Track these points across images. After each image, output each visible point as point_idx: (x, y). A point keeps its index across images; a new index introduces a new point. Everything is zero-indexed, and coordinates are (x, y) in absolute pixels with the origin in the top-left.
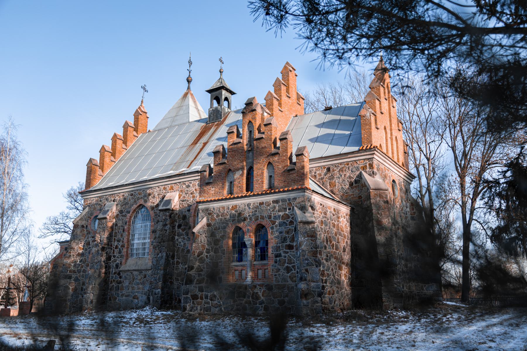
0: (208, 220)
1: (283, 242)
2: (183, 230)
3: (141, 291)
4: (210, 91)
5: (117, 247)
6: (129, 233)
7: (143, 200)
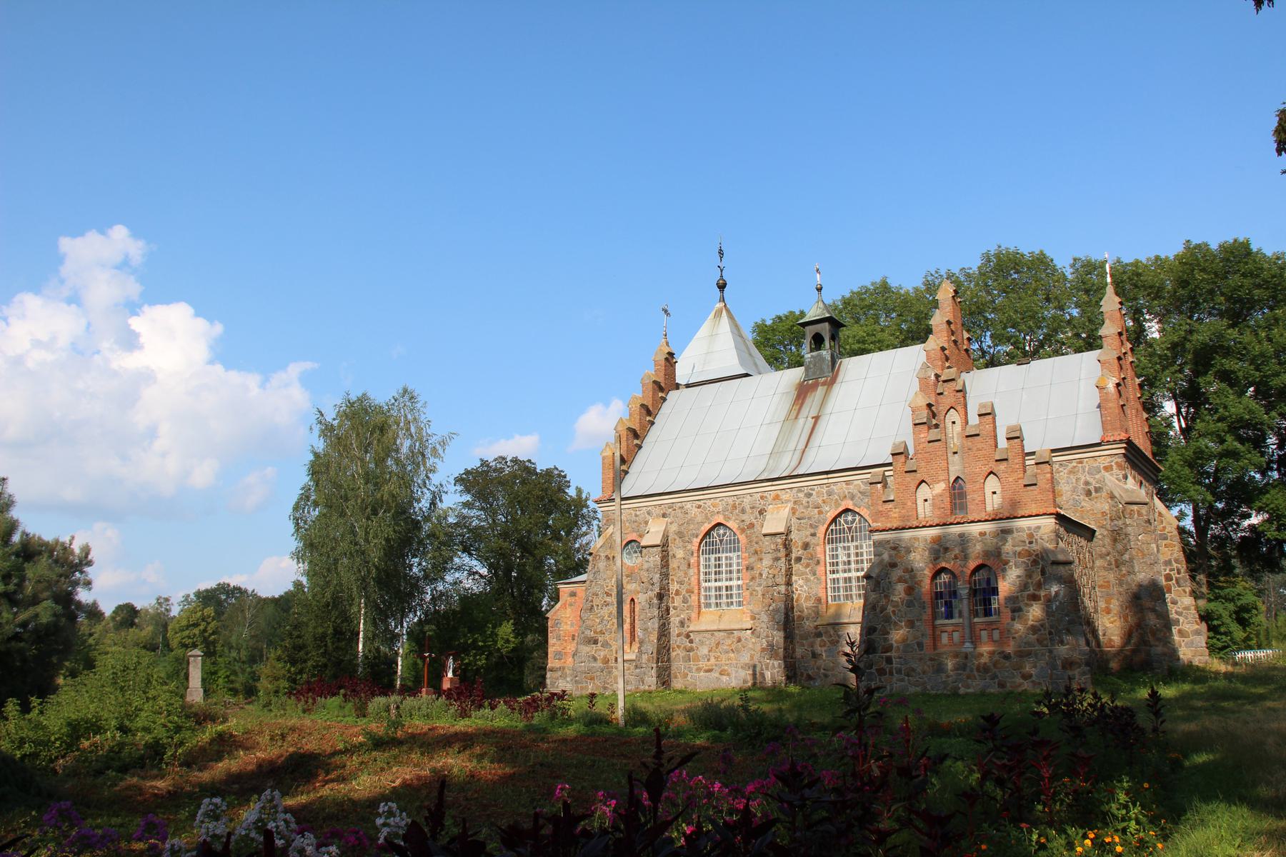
2: (808, 565)
5: (677, 593)
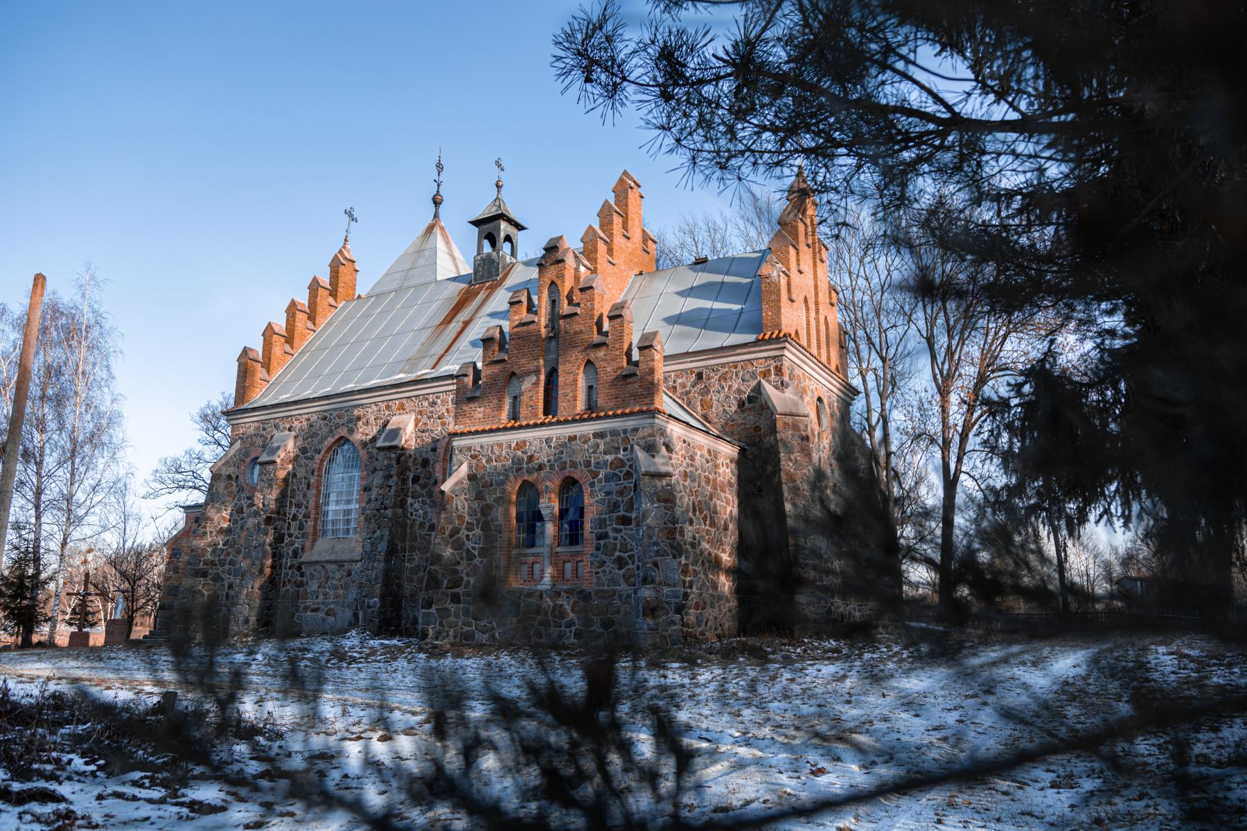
0: (470, 467)
1: (611, 512)
2: (423, 487)
3: (341, 600)
4: (476, 223)
5: (295, 518)
6: (319, 491)
7: (345, 430)
